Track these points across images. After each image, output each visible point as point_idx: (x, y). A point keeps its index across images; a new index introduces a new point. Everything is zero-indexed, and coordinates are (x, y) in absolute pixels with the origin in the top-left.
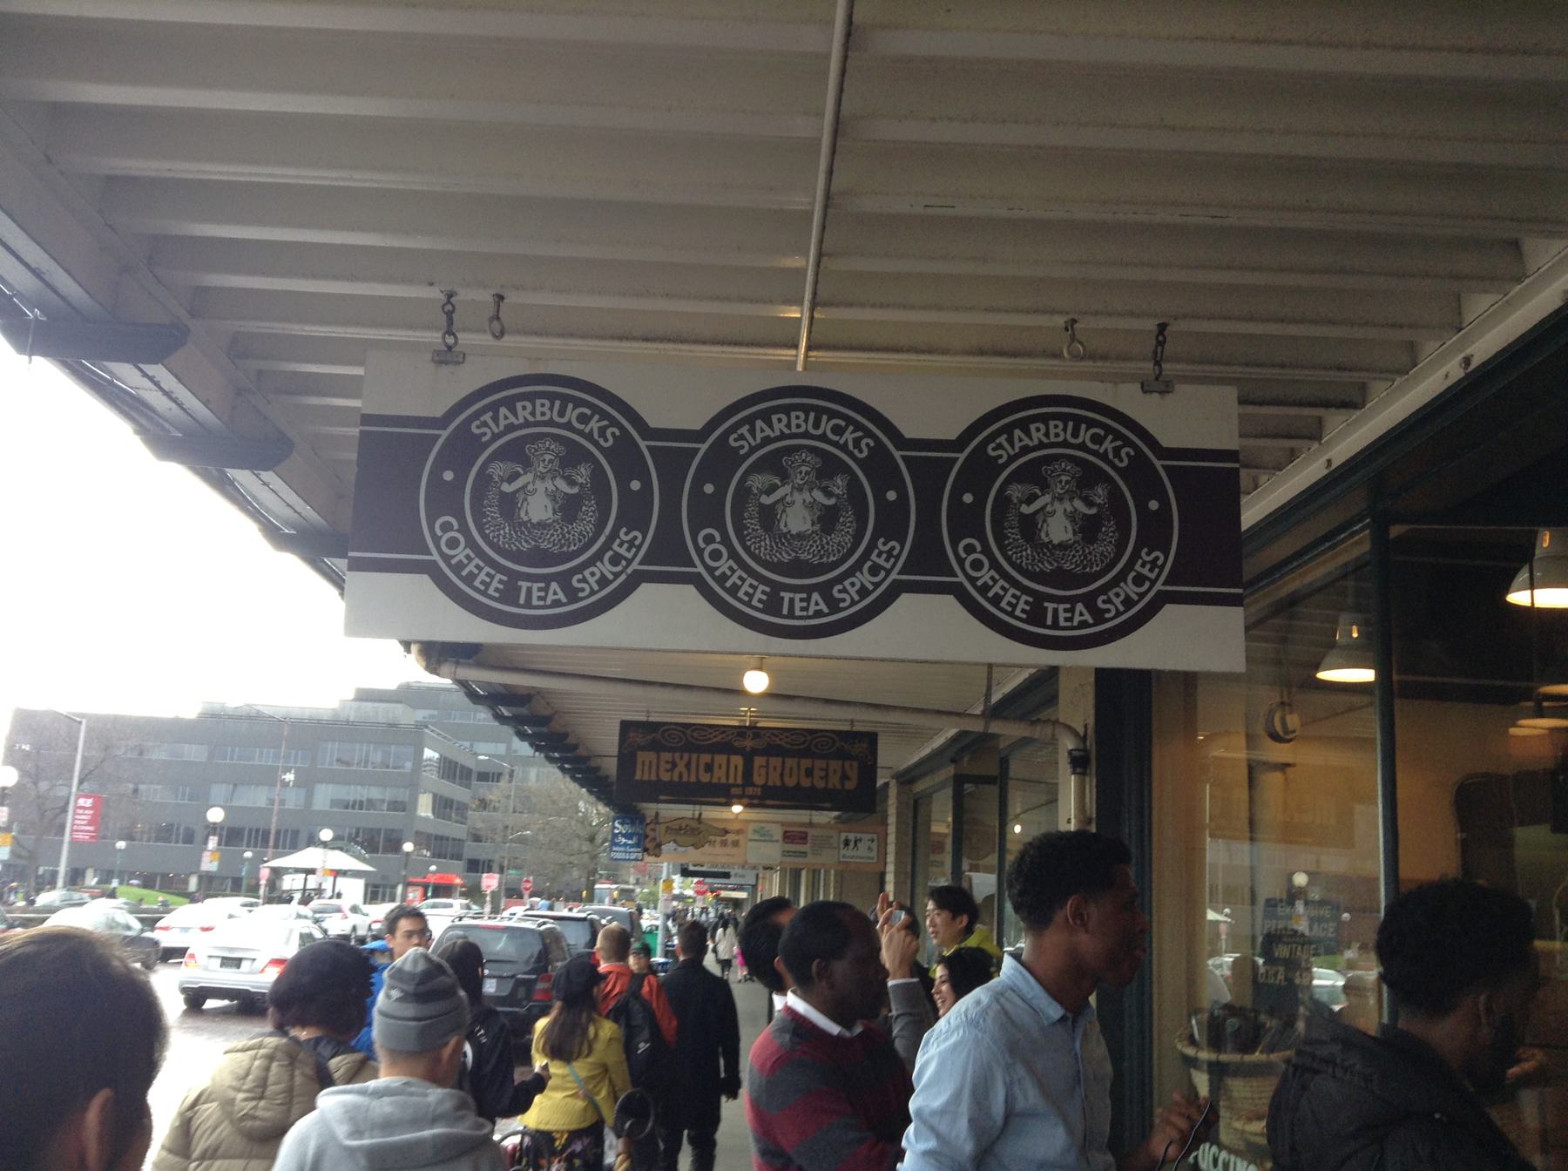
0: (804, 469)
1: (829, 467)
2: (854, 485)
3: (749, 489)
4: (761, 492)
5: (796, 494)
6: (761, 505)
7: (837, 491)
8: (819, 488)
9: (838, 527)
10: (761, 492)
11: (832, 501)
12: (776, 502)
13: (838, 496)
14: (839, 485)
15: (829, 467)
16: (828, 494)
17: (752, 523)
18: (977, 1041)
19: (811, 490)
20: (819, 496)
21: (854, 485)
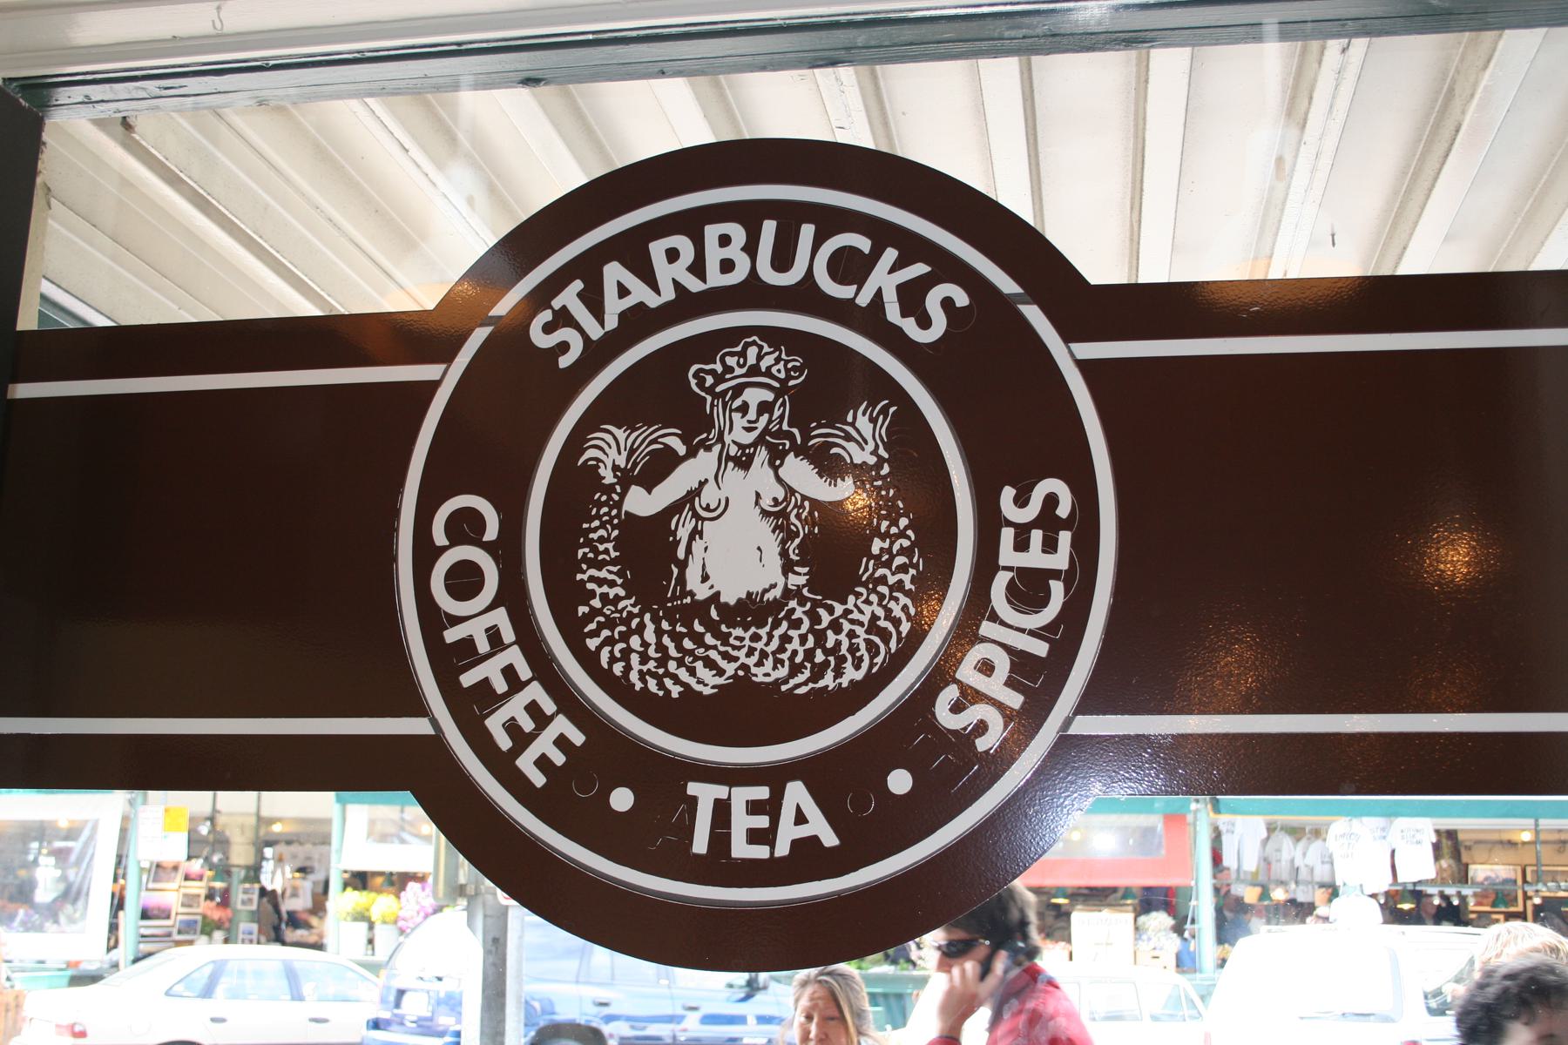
0: (754, 396)
1: (824, 390)
2: (908, 435)
3: (592, 471)
4: (626, 479)
5: (732, 474)
7: (861, 456)
8: (801, 451)
9: (867, 569)
10: (626, 479)
12: (676, 508)
14: (863, 436)
15: (824, 390)
16: (829, 466)
17: (604, 582)
19: (777, 458)
20: (799, 472)
21: (908, 435)
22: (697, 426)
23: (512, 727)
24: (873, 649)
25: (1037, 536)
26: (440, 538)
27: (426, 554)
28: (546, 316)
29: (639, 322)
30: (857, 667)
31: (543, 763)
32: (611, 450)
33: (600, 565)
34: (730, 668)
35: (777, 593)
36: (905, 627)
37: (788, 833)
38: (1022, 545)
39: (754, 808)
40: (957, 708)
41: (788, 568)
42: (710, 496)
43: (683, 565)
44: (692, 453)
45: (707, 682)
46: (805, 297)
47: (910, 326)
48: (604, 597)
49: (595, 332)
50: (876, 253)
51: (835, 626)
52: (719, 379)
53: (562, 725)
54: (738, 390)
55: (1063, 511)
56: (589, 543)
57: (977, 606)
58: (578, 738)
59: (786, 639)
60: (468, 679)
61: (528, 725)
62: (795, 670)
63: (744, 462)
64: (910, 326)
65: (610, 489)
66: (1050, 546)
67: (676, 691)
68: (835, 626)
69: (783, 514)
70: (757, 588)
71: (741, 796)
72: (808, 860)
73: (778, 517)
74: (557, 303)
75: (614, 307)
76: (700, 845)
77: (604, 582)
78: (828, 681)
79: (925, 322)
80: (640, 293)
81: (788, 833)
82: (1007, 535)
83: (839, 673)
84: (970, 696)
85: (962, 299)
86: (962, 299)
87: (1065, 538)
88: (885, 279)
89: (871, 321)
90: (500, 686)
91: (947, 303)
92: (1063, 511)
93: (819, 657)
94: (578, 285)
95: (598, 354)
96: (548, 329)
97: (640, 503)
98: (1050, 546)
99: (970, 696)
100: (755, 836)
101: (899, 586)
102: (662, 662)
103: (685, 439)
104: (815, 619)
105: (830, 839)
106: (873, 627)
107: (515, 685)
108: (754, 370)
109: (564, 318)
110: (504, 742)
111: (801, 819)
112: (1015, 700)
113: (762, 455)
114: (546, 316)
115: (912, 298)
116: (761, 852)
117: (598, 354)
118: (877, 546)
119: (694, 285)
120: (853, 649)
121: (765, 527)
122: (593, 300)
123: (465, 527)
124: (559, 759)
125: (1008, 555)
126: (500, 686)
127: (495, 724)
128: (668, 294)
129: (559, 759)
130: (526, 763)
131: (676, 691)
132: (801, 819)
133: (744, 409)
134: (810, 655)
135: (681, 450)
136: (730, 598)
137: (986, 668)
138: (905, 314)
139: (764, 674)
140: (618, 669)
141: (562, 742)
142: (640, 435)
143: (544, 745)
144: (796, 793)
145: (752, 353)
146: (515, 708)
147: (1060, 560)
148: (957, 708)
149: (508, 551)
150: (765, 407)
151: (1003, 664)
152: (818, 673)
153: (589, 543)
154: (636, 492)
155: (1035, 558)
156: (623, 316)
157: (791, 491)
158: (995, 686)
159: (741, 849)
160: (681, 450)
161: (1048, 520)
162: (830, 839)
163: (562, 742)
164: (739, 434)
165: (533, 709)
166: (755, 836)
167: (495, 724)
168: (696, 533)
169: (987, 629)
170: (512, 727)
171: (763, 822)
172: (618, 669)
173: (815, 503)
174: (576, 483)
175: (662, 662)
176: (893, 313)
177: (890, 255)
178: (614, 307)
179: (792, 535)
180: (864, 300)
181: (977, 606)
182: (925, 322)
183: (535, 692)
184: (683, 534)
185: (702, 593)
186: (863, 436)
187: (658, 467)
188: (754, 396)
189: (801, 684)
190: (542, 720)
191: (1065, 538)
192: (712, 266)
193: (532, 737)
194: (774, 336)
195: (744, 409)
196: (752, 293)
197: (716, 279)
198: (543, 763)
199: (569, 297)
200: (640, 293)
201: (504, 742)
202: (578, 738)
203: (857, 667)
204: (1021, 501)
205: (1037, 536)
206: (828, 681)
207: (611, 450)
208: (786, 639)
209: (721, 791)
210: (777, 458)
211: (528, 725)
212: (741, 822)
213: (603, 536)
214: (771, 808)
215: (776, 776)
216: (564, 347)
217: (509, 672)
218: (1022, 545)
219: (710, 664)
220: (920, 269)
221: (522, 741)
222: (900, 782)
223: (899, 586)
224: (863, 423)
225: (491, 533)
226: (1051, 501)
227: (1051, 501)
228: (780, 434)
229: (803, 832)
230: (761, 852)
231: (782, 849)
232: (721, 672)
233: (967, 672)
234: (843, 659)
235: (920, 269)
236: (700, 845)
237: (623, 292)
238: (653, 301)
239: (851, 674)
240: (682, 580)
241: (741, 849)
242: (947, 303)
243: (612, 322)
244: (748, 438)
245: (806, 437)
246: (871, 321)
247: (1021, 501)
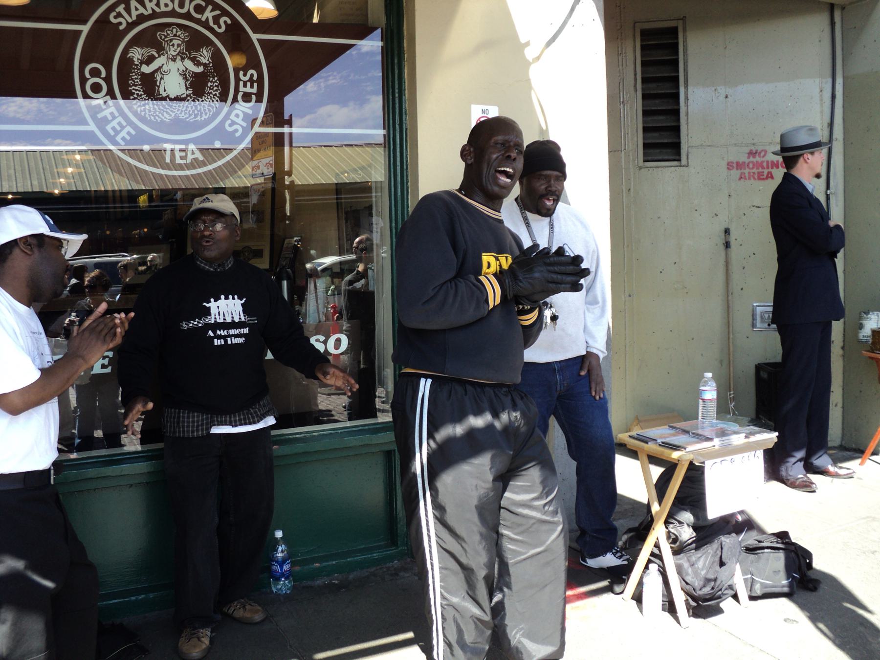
1: (195, 42)
3: (131, 60)
5: (171, 63)
6: (143, 75)
7: (205, 61)
8: (190, 58)
9: (207, 90)
10: (142, 63)
11: (201, 69)
12: (156, 71)
13: (205, 65)
14: (205, 56)
15: (195, 42)
18: (571, 531)
19: (182, 59)
20: (189, 64)
22: (160, 50)
23: (113, 128)
24: (210, 111)
25: (249, 84)
26: (87, 75)
27: (83, 80)
28: (114, 14)
29: (141, 19)
30: (206, 114)
31: (123, 139)
32: (136, 54)
33: (136, 86)
34: (173, 115)
35: (184, 96)
38: (245, 86)
40: (230, 125)
41: (187, 89)
42: (165, 68)
43: (159, 87)
44: (159, 56)
45: (167, 118)
46: (188, 16)
47: (215, 27)
48: (138, 95)
49: (130, 20)
50: (206, 6)
52: (166, 37)
53: (128, 129)
54: (171, 40)
55: (255, 78)
56: (132, 79)
58: (133, 132)
59: (187, 107)
60: (100, 116)
61: (118, 128)
62: (190, 115)
63: (174, 60)
64: (215, 27)
65: (137, 65)
66: (252, 87)
67: (159, 120)
69: (185, 75)
70: (179, 94)
72: (195, 164)
73: (184, 75)
74: (117, 10)
75: (134, 14)
76: (168, 160)
77: (137, 89)
78: (198, 118)
79: (220, 27)
80: (142, 10)
82: (241, 83)
83: (201, 116)
84: (233, 123)
85: (229, 22)
86: (229, 22)
87: (255, 85)
88: (209, 14)
89: (205, 25)
90: (110, 118)
91: (225, 22)
92: (255, 78)
94: (123, 6)
95: (131, 26)
96: (115, 17)
97: (146, 69)
98: (252, 87)
99: (233, 123)
100: (181, 158)
101: (215, 95)
102: (155, 112)
103: (158, 53)
107: (114, 118)
108: (175, 35)
109: (119, 15)
110: (112, 133)
112: (245, 124)
113: (179, 58)
114: (114, 14)
115: (216, 19)
117: (131, 26)
118: (210, 84)
119: (157, 10)
120: (205, 110)
121: (181, 78)
122: (128, 10)
123: (95, 73)
124: (128, 138)
125: (241, 88)
126: (110, 118)
127: (109, 128)
128: (150, 12)
129: (128, 138)
130: (118, 138)
131: (159, 120)
133: (173, 45)
134: (193, 111)
135: (157, 55)
136: (172, 96)
137: (237, 116)
138: (214, 24)
139: (182, 116)
140: (143, 114)
141: (129, 133)
142: (144, 50)
143: (123, 134)
145: (174, 30)
146: (114, 123)
147: (254, 90)
148: (230, 125)
149: (108, 80)
150: (179, 45)
151: (241, 115)
152: (196, 116)
153: (132, 79)
154: (144, 66)
155: (248, 89)
156: (137, 16)
158: (239, 120)
159: (178, 161)
160: (157, 55)
161: (251, 79)
163: (129, 133)
164: (172, 52)
165: (119, 124)
166: (181, 158)
167: (109, 128)
168: (162, 78)
170: (113, 128)
172: (143, 114)
174: (126, 64)
175: (155, 112)
176: (211, 23)
177: (210, 7)
178: (134, 14)
179: (187, 80)
180: (204, 19)
182: (220, 27)
183: (120, 119)
184: (158, 78)
185: (164, 95)
186: (205, 56)
187: (150, 60)
189: (191, 119)
190: (123, 128)
191: (255, 85)
192: (162, 5)
193: (121, 131)
194: (180, 26)
195: (173, 45)
196: (173, 14)
197: (163, 9)
198: (123, 139)
199: (121, 9)
200: (142, 10)
201: (112, 133)
202: (133, 132)
203: (206, 114)
204: (245, 75)
205: (249, 84)
206: (198, 118)
207: (136, 54)
210: (182, 59)
211: (118, 128)
212: (178, 155)
213: (136, 78)
216: (120, 23)
217: (112, 114)
218: (245, 86)
219: (167, 112)
220: (218, 12)
221: (117, 133)
223: (215, 95)
224: (205, 52)
225: (103, 75)
226: (252, 75)
227: (252, 75)
228: (183, 53)
229: (194, 156)
231: (189, 161)
233: (232, 117)
234: (202, 113)
235: (218, 12)
236: (168, 160)
237: (137, 9)
238: (146, 13)
239: (204, 117)
240: (158, 91)
241: (178, 161)
242: (225, 22)
243: (134, 18)
244: (175, 54)
245: (190, 54)
246: (205, 25)
247: (245, 75)
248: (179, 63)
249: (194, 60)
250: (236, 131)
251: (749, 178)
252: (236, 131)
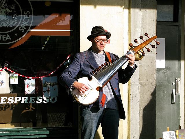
5: (2, 9)
11: (11, 11)
16: (10, 9)
19: (6, 8)
20: (8, 10)
36: (16, 22)
37: (7, 38)
39: (4, 37)
51: (11, 22)
54: (2, 2)
57: (22, 21)
59: (7, 23)
63: (3, 8)
68: (11, 22)
71: (3, 36)
81: (7, 38)
93: (10, 25)
100: (4, 39)
104: (9, 22)
105: (11, 39)
106: (14, 22)
111: (8, 37)
112: (25, 29)
116: (5, 40)
132: (8, 37)
144: (8, 35)
150: (5, 4)
157: (7, 11)
159: (3, 40)
162: (11, 39)
166: (4, 39)
169: (23, 23)
171: (5, 38)
173: (10, 12)
181: (22, 21)
188: (4, 3)
208: (7, 23)
209: (2, 35)
210: (6, 8)
212: (3, 38)
214: (6, 37)
215: (6, 34)
222: (16, 35)
226: (28, 13)
227: (28, 13)
228: (6, 6)
229: (8, 38)
230: (5, 40)
231: (7, 40)
232: (1, 26)
241: (3, 40)
247: (26, 13)
248: (4, 10)
249: (9, 8)
250: (22, 30)
251: (128, 52)
252: (22, 30)
